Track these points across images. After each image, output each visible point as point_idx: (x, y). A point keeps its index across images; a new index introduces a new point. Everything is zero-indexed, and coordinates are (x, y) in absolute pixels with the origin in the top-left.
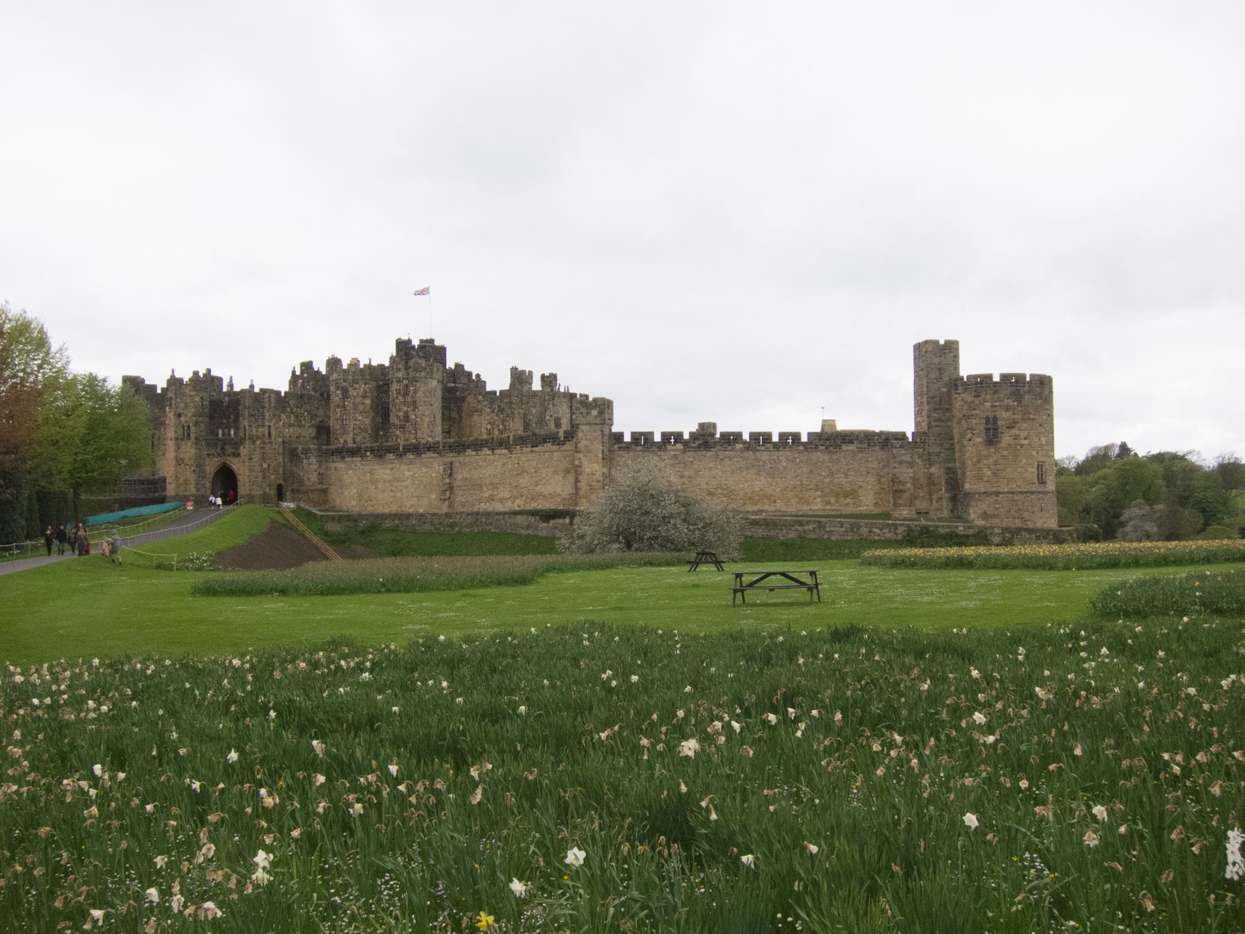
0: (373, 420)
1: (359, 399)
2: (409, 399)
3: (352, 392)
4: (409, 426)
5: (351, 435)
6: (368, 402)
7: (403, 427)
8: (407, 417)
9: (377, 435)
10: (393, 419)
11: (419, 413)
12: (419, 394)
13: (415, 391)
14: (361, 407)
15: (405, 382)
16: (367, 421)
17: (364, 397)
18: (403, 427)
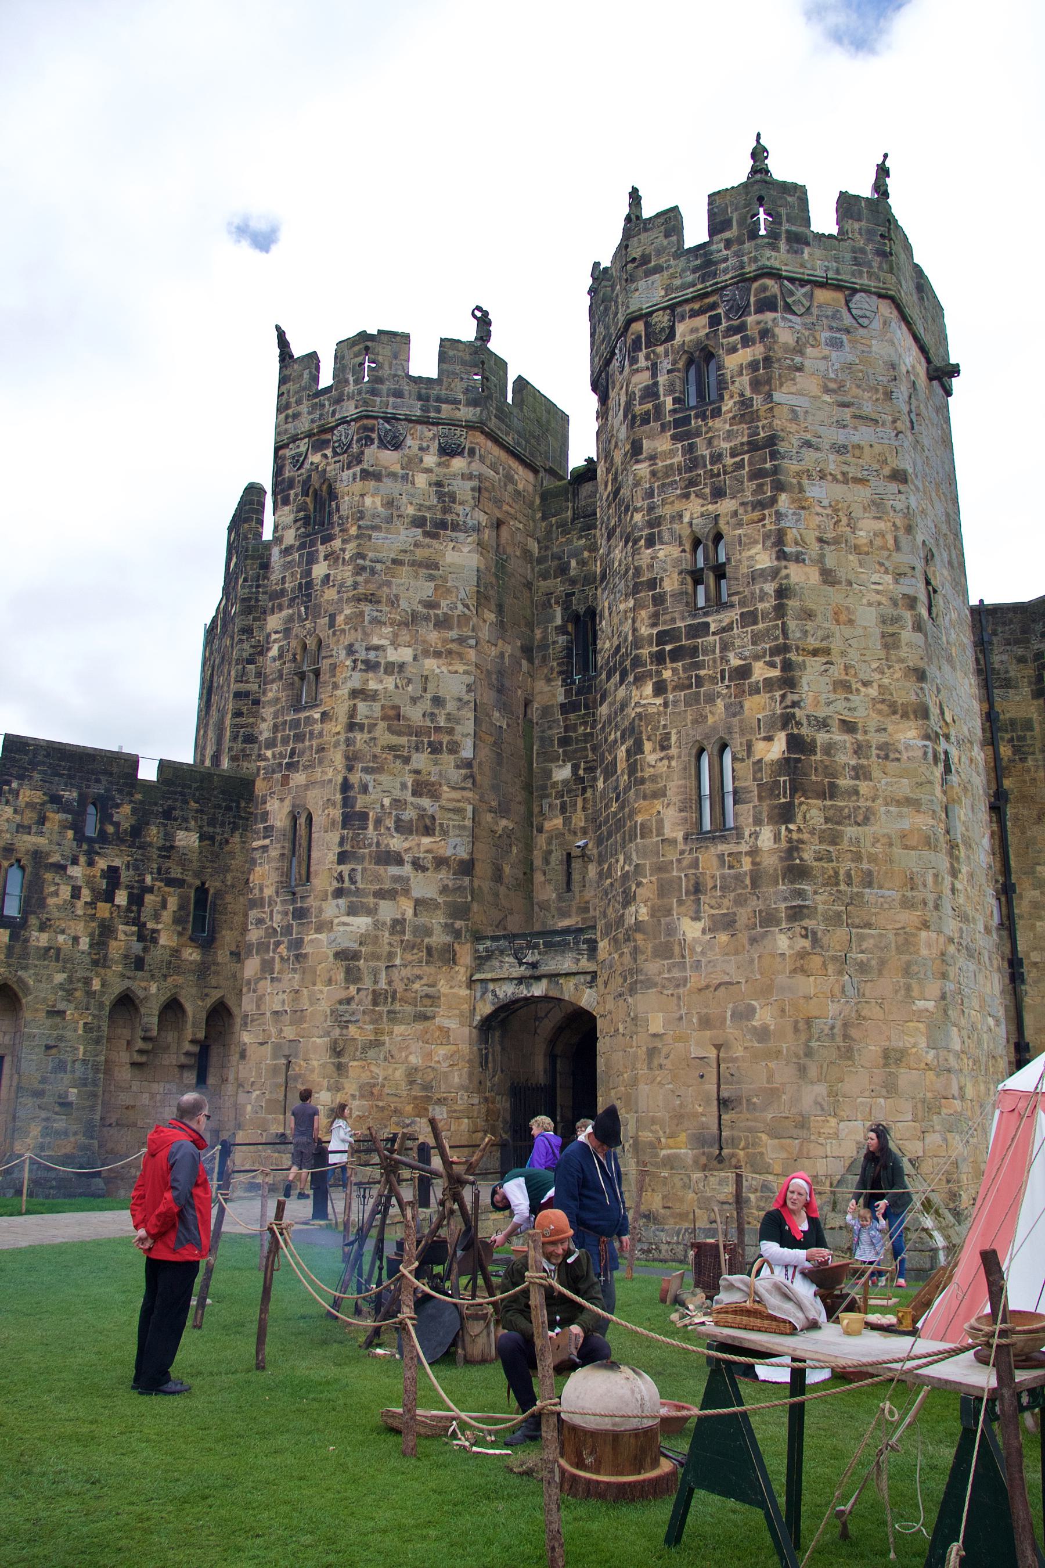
0: (499, 680)
1: (399, 539)
2: (723, 433)
3: (350, 489)
4: (734, 641)
5: (333, 770)
6: (462, 558)
7: (677, 648)
8: (709, 571)
9: (534, 787)
10: (622, 622)
11: (802, 530)
12: (800, 397)
13: (764, 375)
14: (412, 590)
15: (689, 331)
16: (453, 680)
17: (437, 525)
18: (677, 648)
